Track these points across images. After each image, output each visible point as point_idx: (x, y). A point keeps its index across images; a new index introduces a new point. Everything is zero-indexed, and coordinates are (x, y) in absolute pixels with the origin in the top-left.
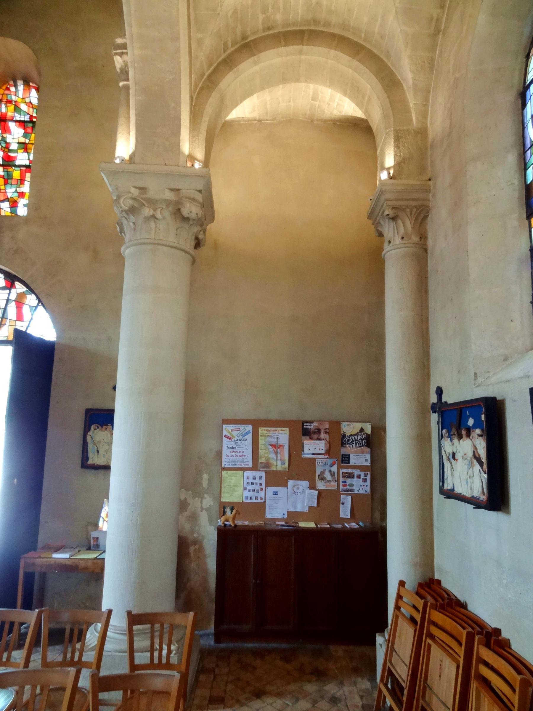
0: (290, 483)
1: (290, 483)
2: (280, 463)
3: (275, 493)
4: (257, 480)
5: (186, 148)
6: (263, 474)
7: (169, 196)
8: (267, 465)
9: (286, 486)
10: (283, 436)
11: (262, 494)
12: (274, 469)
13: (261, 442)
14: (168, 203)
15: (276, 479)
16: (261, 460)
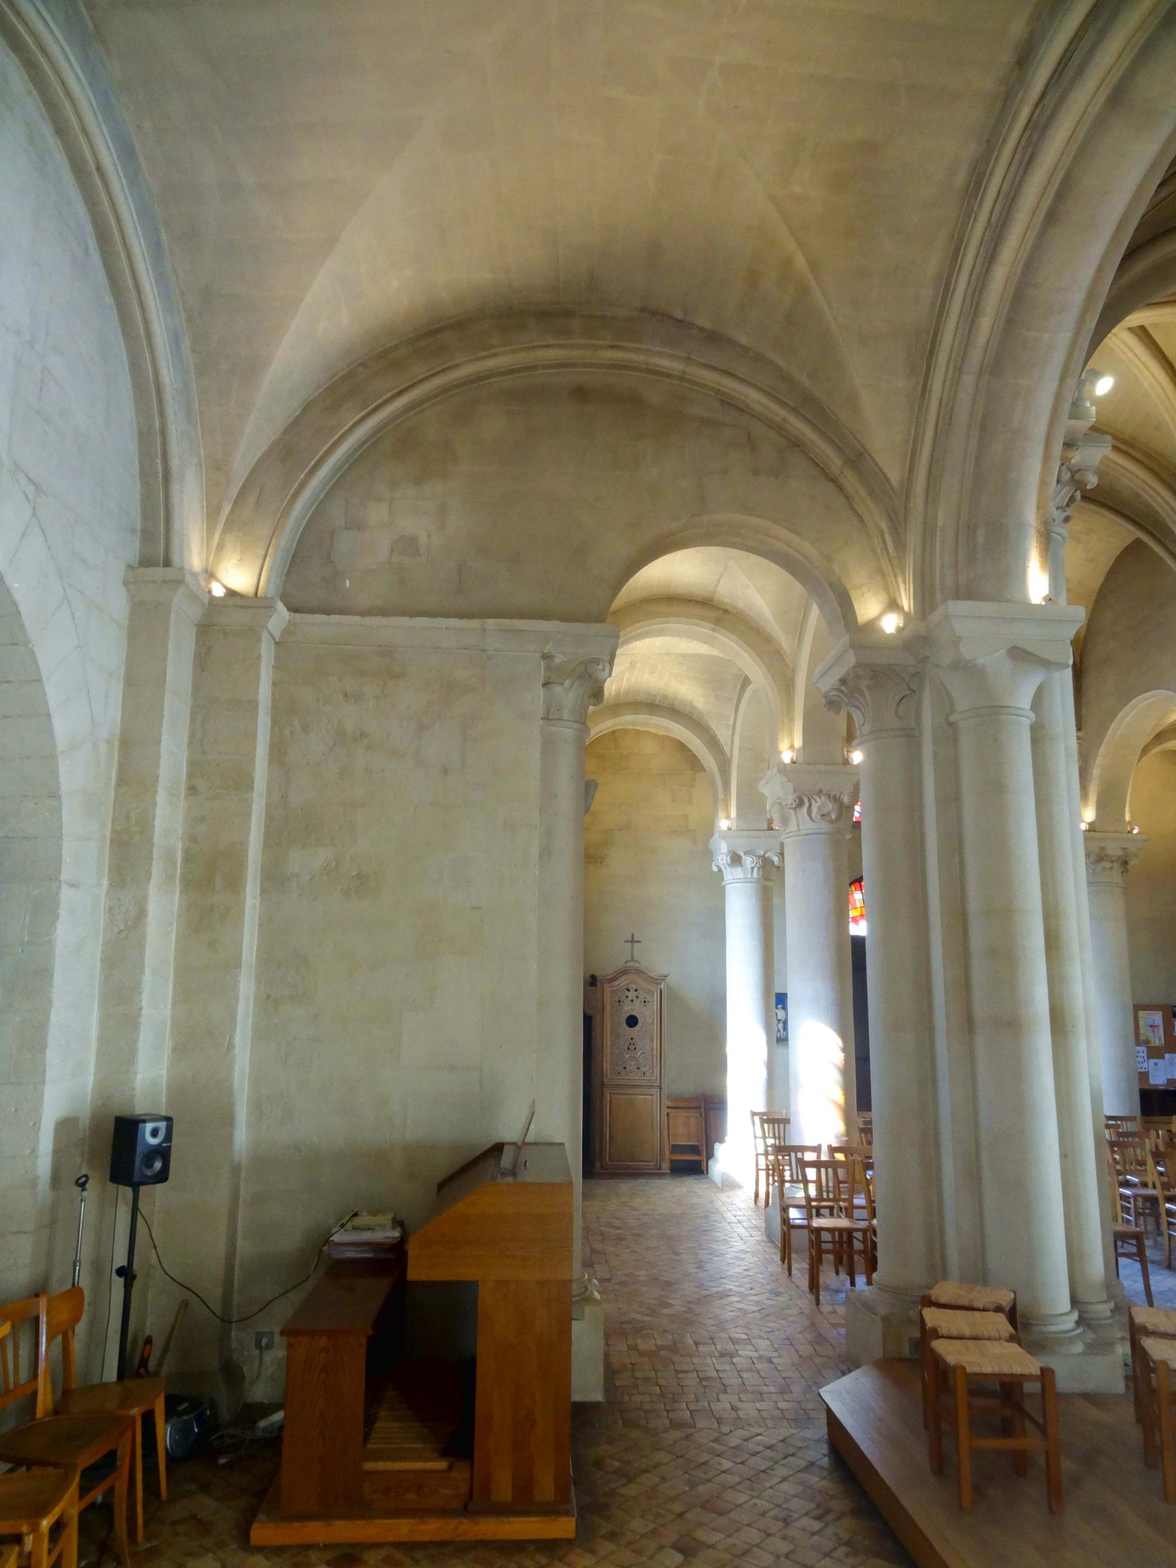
0: (1167, 1056)
1: (1167, 1056)
2: (1158, 1040)
3: (1156, 1064)
4: (1141, 1054)
5: (1128, 818)
6: (1144, 1048)
7: (1120, 853)
8: (1147, 1042)
9: (1163, 1058)
10: (1158, 1018)
11: (1145, 1065)
12: (1152, 1044)
13: (1141, 1023)
14: (1120, 857)
15: (1155, 1053)
16: (1142, 1038)
